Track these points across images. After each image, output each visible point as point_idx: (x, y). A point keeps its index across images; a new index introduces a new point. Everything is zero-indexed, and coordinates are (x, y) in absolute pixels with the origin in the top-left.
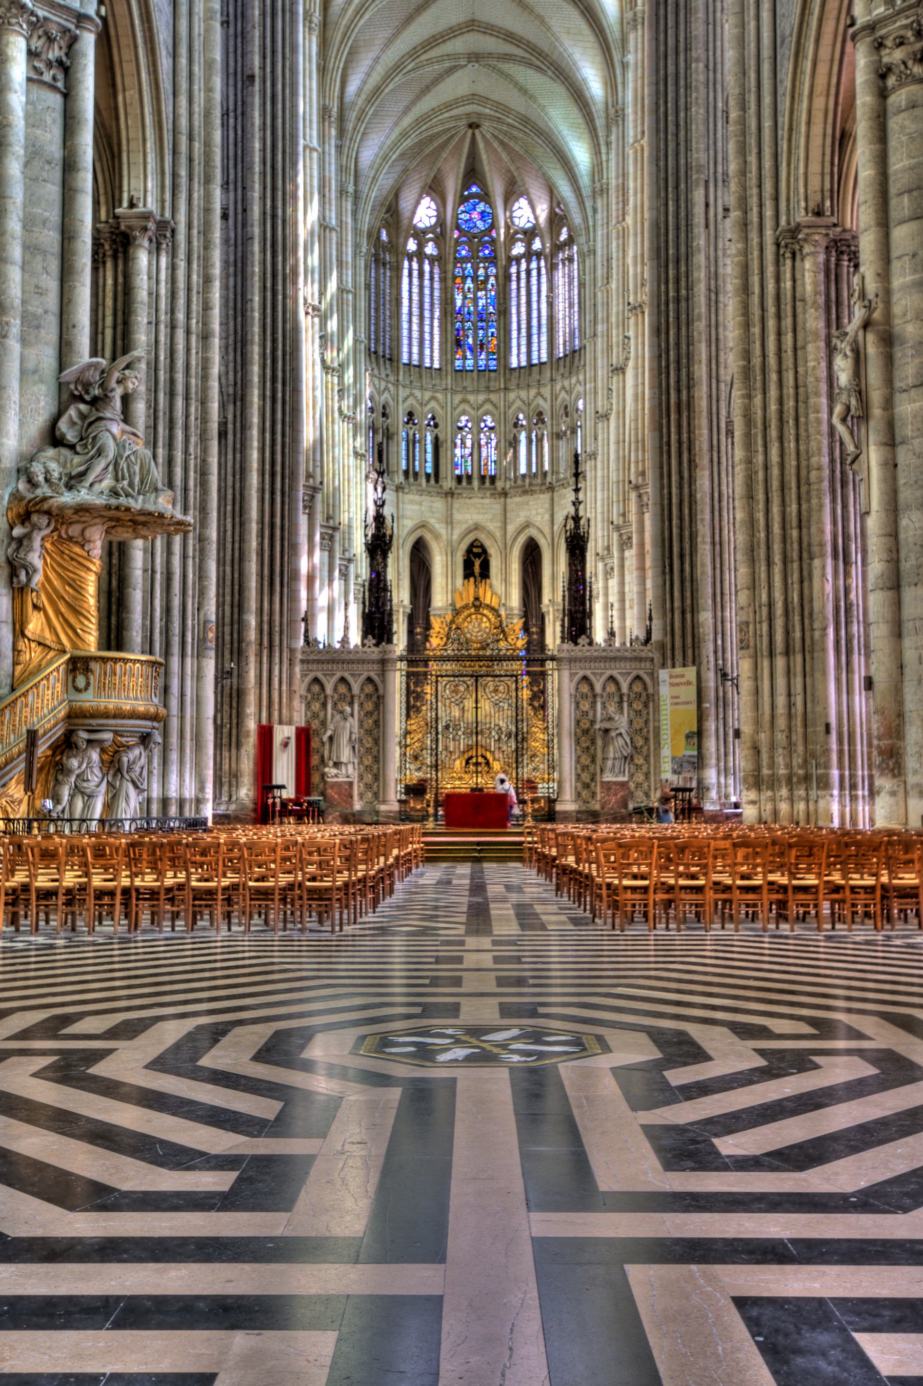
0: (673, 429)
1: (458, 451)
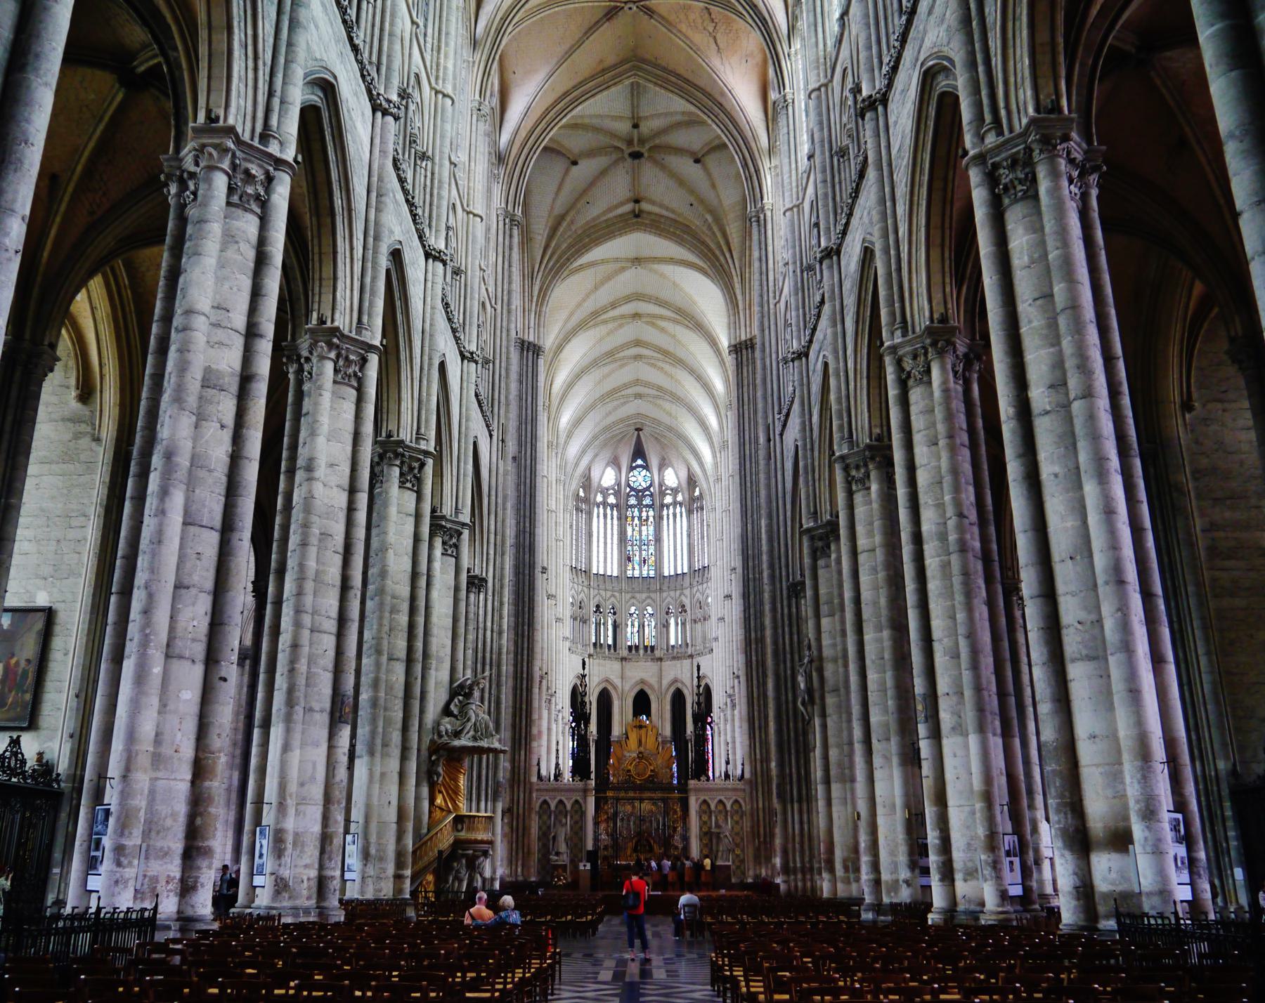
0: (753, 653)
1: (629, 629)
